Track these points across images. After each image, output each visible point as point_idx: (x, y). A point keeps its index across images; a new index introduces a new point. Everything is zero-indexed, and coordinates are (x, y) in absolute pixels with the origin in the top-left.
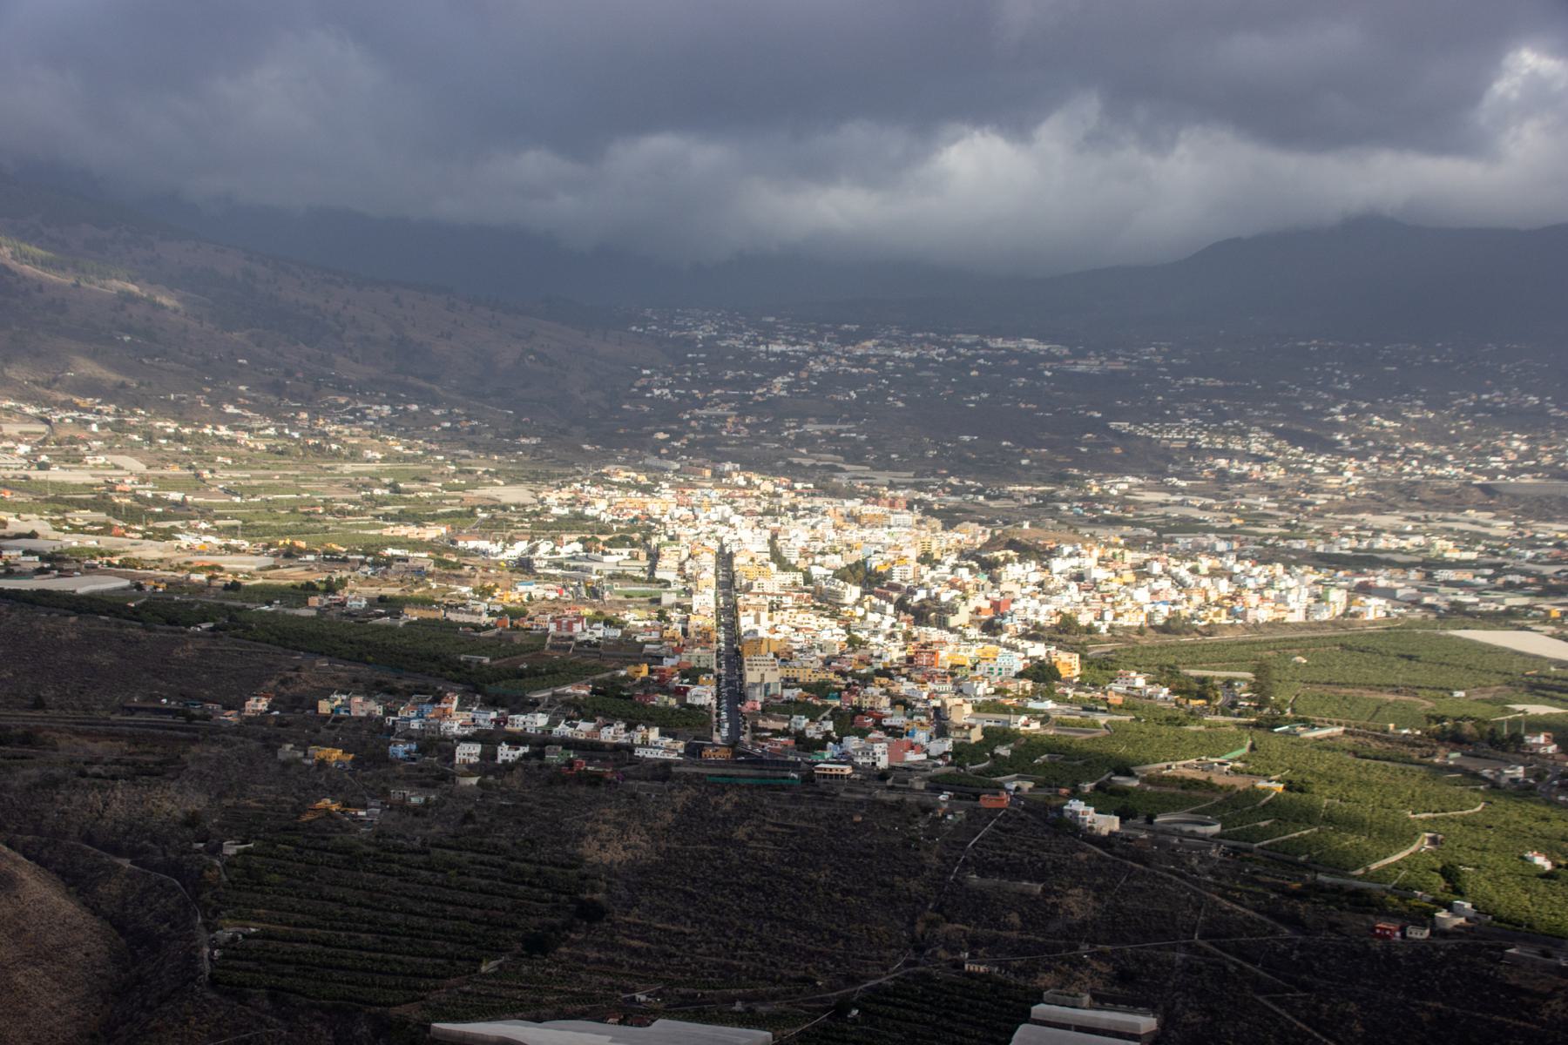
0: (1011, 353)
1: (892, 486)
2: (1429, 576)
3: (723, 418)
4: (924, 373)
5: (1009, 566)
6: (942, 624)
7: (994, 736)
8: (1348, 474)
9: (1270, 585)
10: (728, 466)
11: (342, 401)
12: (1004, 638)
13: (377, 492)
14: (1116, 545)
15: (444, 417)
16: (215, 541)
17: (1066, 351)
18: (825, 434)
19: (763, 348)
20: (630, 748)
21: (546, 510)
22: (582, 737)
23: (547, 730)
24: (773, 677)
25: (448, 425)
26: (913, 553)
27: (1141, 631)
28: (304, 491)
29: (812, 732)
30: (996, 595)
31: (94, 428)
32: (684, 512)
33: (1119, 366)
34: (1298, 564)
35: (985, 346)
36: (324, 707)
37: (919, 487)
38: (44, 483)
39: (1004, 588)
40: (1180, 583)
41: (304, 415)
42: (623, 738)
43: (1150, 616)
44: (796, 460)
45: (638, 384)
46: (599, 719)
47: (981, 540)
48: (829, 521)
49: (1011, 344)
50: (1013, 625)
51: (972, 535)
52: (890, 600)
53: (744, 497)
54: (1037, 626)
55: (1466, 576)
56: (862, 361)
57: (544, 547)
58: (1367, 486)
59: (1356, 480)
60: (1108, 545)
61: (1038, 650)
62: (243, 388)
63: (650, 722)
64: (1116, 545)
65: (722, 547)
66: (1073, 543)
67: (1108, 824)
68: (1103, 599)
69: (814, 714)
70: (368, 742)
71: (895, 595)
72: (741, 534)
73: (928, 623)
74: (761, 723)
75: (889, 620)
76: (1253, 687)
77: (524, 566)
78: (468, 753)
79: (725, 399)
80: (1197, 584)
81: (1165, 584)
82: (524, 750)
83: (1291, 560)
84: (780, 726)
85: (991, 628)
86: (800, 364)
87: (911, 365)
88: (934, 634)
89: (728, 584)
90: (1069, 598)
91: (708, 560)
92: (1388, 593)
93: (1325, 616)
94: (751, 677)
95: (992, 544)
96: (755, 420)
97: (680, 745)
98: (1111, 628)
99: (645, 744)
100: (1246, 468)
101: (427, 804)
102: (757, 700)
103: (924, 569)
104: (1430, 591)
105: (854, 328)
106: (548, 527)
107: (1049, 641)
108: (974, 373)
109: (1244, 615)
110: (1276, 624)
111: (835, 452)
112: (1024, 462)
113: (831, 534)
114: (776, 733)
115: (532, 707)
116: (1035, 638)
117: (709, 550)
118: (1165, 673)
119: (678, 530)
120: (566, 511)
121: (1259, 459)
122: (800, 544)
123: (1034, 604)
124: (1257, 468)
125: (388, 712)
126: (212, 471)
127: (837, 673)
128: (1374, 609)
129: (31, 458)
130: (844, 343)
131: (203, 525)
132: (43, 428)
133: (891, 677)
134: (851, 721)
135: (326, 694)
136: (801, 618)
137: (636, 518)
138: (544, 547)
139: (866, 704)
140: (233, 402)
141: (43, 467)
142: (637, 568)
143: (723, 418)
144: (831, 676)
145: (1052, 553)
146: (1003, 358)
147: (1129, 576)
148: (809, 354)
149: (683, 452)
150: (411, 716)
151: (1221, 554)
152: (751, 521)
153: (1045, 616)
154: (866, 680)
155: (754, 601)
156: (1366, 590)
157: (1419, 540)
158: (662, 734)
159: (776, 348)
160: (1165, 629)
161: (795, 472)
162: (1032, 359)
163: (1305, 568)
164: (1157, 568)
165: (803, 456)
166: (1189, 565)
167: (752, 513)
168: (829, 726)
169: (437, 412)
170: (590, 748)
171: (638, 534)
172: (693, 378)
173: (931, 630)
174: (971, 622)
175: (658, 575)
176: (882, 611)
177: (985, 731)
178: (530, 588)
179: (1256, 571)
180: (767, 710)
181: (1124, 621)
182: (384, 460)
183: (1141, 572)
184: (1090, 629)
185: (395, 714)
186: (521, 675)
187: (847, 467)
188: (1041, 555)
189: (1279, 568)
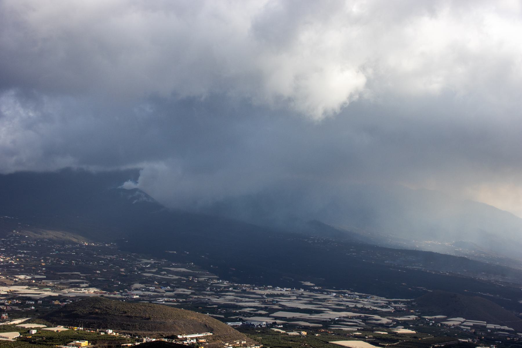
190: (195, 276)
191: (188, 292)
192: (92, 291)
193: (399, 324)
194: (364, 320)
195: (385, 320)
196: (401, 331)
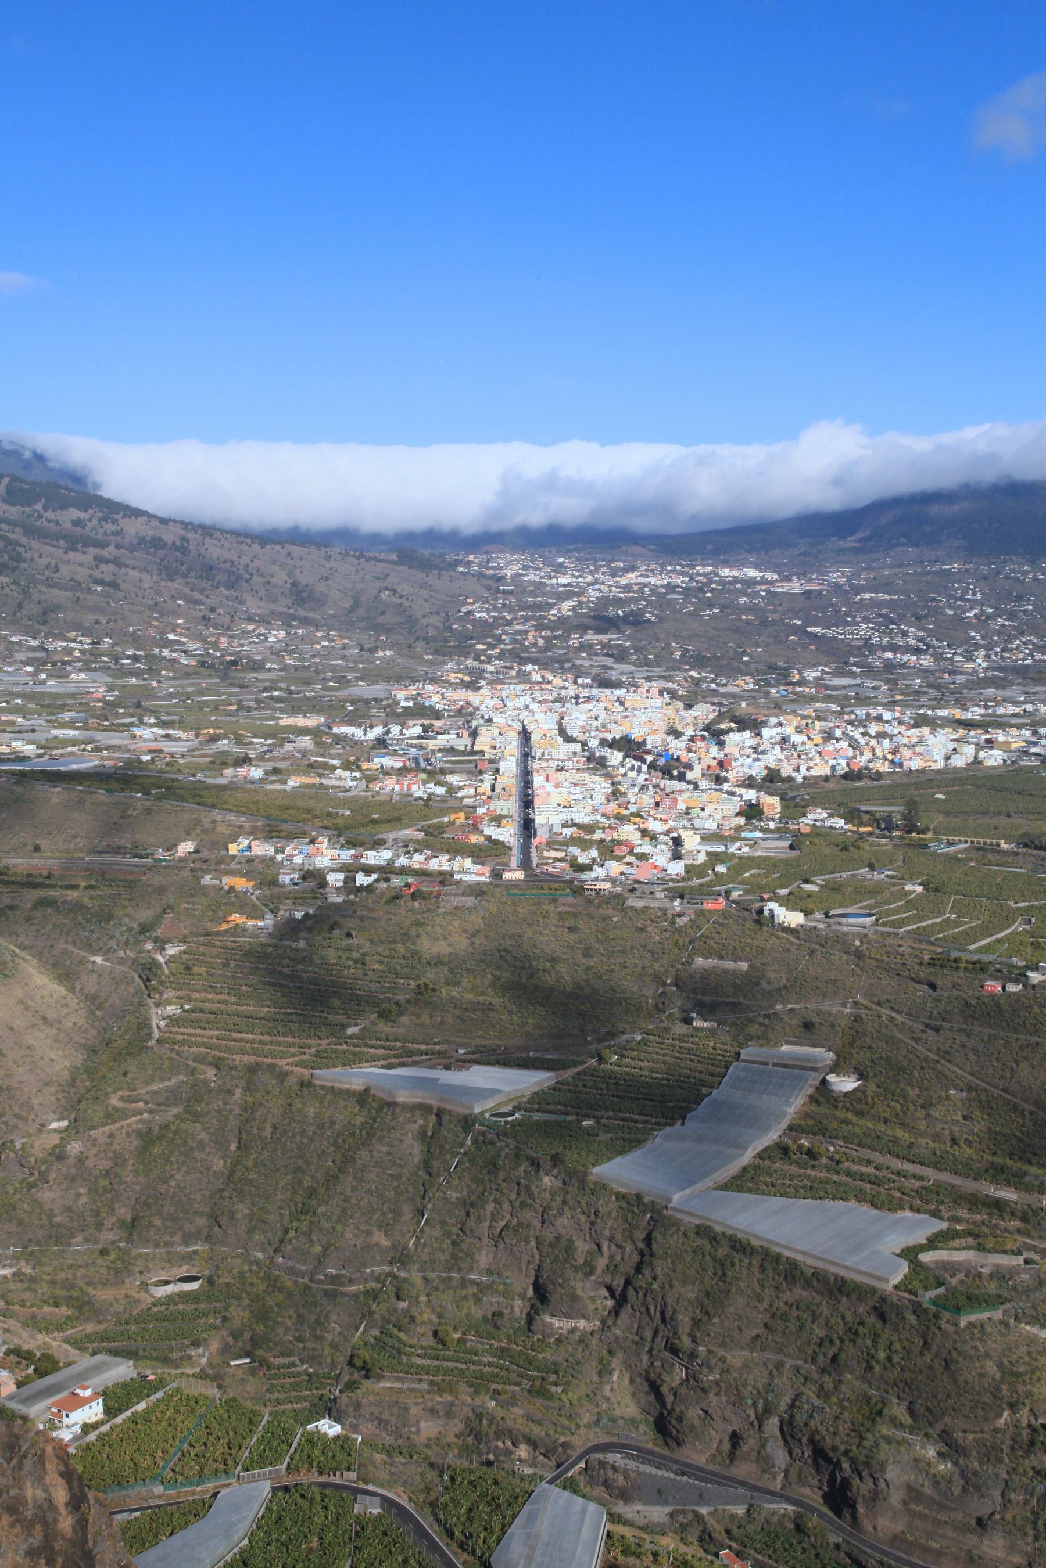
0: (736, 580)
1: (648, 679)
2: (1035, 733)
3: (526, 632)
4: (674, 596)
5: (731, 734)
6: (681, 777)
7: (714, 858)
8: (979, 661)
9: (921, 742)
10: (529, 668)
11: (250, 628)
12: (726, 787)
13: (276, 693)
14: (809, 717)
15: (324, 638)
16: (160, 732)
17: (776, 577)
18: (600, 642)
19: (554, 581)
20: (451, 874)
21: (398, 703)
22: (416, 866)
23: (390, 862)
25: (326, 643)
26: (663, 727)
27: (826, 779)
28: (224, 694)
29: (583, 859)
30: (721, 756)
31: (77, 653)
32: (496, 701)
33: (813, 587)
34: (942, 727)
35: (717, 575)
36: (233, 849)
37: (669, 679)
38: (43, 693)
39: (726, 750)
41: (223, 639)
42: (446, 867)
43: (833, 768)
44: (578, 662)
45: (464, 609)
46: (429, 852)
47: (712, 716)
48: (602, 705)
49: (735, 573)
51: (704, 712)
52: (644, 761)
53: (541, 689)
54: (751, 777)
56: (627, 588)
57: (395, 730)
58: (993, 669)
59: (985, 665)
60: (804, 717)
61: (751, 795)
62: (180, 621)
64: (809, 717)
65: (524, 727)
66: (777, 716)
68: (799, 756)
69: (585, 845)
70: (264, 873)
71: (649, 758)
72: (538, 716)
73: (672, 777)
74: (546, 854)
75: (643, 776)
76: (905, 817)
77: (381, 743)
78: (336, 879)
79: (527, 619)
80: (867, 744)
81: (844, 744)
82: (374, 876)
83: (933, 724)
84: (560, 855)
85: (719, 780)
86: (582, 592)
87: (663, 590)
88: (674, 785)
89: (526, 756)
90: (774, 758)
93: (958, 762)
94: (539, 820)
96: (549, 633)
97: (487, 870)
98: (804, 778)
99: (462, 871)
100: (905, 658)
101: (307, 916)
102: (542, 836)
103: (670, 738)
104: (1035, 744)
105: (621, 565)
106: (398, 715)
107: (759, 788)
108: (709, 595)
109: (901, 765)
110: (922, 771)
111: (608, 655)
112: (745, 659)
113: (603, 715)
114: (556, 860)
116: (750, 786)
117: (513, 729)
119: (492, 715)
120: (411, 704)
121: (917, 651)
122: (580, 723)
123: (750, 760)
124: (914, 658)
125: (277, 851)
126: (159, 682)
127: (603, 815)
128: (994, 758)
129: (35, 674)
130: (614, 575)
131: (152, 720)
132: (43, 655)
133: (642, 817)
134: (608, 850)
136: (578, 777)
137: (462, 707)
138: (395, 730)
139: (623, 838)
140: (173, 631)
143: (526, 632)
144: (598, 818)
145: (764, 723)
146: (729, 583)
148: (589, 584)
149: (496, 658)
150: (296, 854)
151: (887, 722)
152: (543, 707)
153: (758, 770)
154: (621, 819)
155: (544, 764)
156: (990, 743)
157: (1029, 707)
158: (474, 863)
159: (564, 580)
161: (578, 673)
162: (750, 583)
163: (947, 730)
164: (838, 733)
165: (583, 658)
166: (862, 730)
167: (546, 701)
168: (594, 853)
169: (319, 634)
170: (423, 874)
172: (504, 605)
173: (674, 782)
174: (703, 775)
175: (476, 748)
176: (639, 771)
177: (708, 854)
178: (382, 760)
179: (909, 733)
180: (550, 845)
181: (815, 772)
182: (280, 670)
183: (829, 736)
184: (790, 779)
185: (283, 852)
186: (374, 822)
187: (615, 666)
188: (754, 726)
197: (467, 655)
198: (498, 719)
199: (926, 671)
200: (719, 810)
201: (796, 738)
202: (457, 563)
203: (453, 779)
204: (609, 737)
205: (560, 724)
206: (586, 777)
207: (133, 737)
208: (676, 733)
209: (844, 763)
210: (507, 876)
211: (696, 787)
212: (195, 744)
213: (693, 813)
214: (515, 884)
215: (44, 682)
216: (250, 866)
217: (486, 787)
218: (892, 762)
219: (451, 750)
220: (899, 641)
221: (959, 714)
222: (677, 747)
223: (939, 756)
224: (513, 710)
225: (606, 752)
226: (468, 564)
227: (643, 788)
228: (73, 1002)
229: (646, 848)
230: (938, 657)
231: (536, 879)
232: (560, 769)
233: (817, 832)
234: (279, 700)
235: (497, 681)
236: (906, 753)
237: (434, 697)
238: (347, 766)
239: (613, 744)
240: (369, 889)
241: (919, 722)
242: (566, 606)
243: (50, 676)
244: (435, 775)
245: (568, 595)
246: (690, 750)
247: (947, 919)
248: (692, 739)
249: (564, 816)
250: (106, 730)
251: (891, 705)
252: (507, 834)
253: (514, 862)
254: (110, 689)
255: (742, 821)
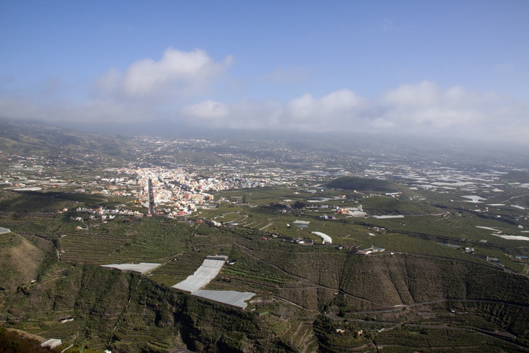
0: (200, 142)
1: (180, 166)
6: (189, 191)
16: (57, 180)
24: (159, 201)
27: (224, 190)
29: (166, 211)
36: (77, 210)
37: (185, 166)
40: (230, 182)
50: (201, 191)
51: (193, 174)
55: (276, 179)
56: (174, 144)
63: (137, 210)
67: (220, 224)
69: (167, 208)
85: (198, 191)
89: (151, 184)
90: (211, 186)
91: (147, 181)
92: (265, 182)
93: (254, 186)
94: (155, 202)
95: (198, 176)
113: (169, 175)
115: (115, 209)
116: (206, 193)
118: (228, 197)
121: (244, 160)
128: (263, 185)
135: (78, 207)
138: (117, 179)
141: (26, 168)
142: (135, 183)
145: (208, 178)
147: (222, 181)
154: (176, 201)
156: (261, 181)
159: (158, 142)
160: (229, 190)
164: (226, 179)
168: (169, 210)
170: (126, 215)
171: (134, 177)
177: (197, 209)
184: (215, 191)
186: (114, 203)
189: (247, 179)
190: (394, 166)
191: (391, 173)
192: (347, 173)
193: (495, 187)
194: (478, 186)
195: (488, 186)
196: (496, 190)
197: (135, 161)
198: (143, 177)
199: (246, 165)
200: (199, 198)
201: (217, 181)
202: (132, 138)
203: (133, 191)
204: (171, 181)
205: (158, 178)
206: (166, 191)
207: (50, 182)
208: (188, 180)
209: (228, 187)
210: (147, 216)
211: (193, 193)
212: (66, 184)
213: (193, 199)
214: (150, 218)
215: (26, 168)
216: (82, 214)
217: (141, 193)
218: (239, 187)
219: (131, 185)
220: (239, 157)
221: (253, 174)
222: (188, 183)
223: (250, 184)
224: (146, 175)
225: (170, 184)
226: (135, 138)
227: (180, 194)
228: (37, 249)
229: (181, 208)
230: (248, 161)
231: (154, 216)
232: (159, 189)
233: (223, 203)
234: (87, 172)
235: (142, 167)
236: (243, 184)
237: (127, 172)
238: (106, 189)
239: (172, 183)
240: (112, 220)
241: (245, 177)
242: (159, 148)
243: (28, 166)
244: (128, 190)
245: (160, 146)
246: (191, 184)
247: (253, 224)
248: (191, 181)
249: (161, 200)
250: (43, 180)
251: (238, 173)
252: (147, 205)
253: (149, 212)
254: (44, 169)
255: (205, 201)
